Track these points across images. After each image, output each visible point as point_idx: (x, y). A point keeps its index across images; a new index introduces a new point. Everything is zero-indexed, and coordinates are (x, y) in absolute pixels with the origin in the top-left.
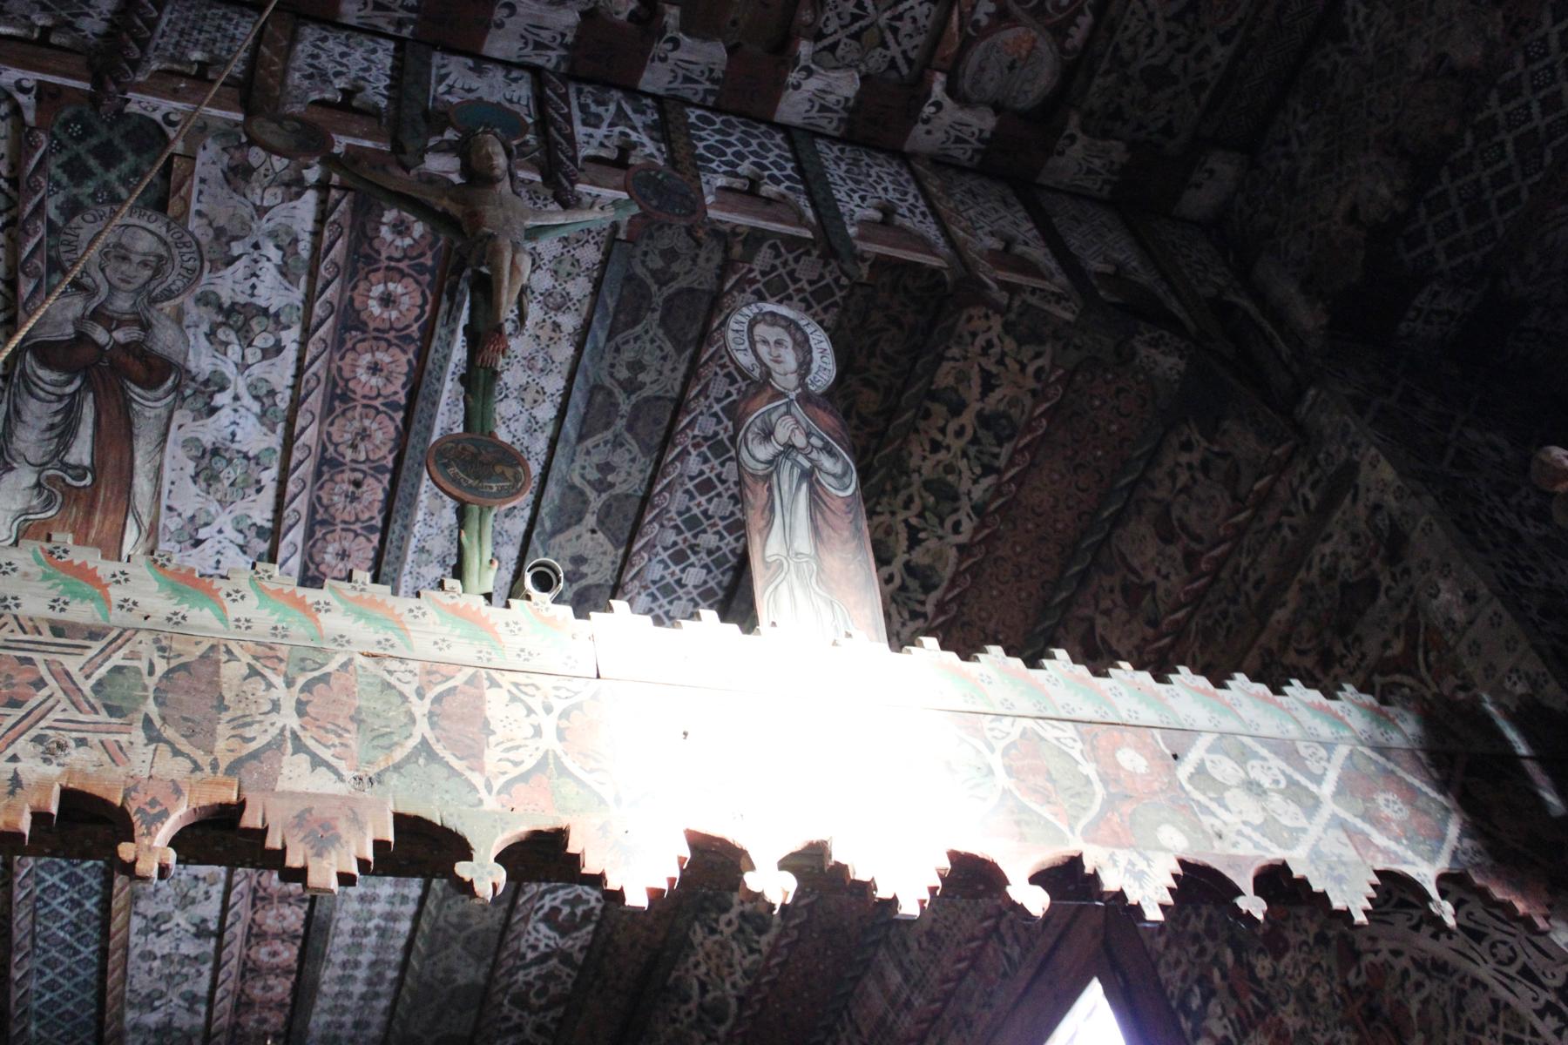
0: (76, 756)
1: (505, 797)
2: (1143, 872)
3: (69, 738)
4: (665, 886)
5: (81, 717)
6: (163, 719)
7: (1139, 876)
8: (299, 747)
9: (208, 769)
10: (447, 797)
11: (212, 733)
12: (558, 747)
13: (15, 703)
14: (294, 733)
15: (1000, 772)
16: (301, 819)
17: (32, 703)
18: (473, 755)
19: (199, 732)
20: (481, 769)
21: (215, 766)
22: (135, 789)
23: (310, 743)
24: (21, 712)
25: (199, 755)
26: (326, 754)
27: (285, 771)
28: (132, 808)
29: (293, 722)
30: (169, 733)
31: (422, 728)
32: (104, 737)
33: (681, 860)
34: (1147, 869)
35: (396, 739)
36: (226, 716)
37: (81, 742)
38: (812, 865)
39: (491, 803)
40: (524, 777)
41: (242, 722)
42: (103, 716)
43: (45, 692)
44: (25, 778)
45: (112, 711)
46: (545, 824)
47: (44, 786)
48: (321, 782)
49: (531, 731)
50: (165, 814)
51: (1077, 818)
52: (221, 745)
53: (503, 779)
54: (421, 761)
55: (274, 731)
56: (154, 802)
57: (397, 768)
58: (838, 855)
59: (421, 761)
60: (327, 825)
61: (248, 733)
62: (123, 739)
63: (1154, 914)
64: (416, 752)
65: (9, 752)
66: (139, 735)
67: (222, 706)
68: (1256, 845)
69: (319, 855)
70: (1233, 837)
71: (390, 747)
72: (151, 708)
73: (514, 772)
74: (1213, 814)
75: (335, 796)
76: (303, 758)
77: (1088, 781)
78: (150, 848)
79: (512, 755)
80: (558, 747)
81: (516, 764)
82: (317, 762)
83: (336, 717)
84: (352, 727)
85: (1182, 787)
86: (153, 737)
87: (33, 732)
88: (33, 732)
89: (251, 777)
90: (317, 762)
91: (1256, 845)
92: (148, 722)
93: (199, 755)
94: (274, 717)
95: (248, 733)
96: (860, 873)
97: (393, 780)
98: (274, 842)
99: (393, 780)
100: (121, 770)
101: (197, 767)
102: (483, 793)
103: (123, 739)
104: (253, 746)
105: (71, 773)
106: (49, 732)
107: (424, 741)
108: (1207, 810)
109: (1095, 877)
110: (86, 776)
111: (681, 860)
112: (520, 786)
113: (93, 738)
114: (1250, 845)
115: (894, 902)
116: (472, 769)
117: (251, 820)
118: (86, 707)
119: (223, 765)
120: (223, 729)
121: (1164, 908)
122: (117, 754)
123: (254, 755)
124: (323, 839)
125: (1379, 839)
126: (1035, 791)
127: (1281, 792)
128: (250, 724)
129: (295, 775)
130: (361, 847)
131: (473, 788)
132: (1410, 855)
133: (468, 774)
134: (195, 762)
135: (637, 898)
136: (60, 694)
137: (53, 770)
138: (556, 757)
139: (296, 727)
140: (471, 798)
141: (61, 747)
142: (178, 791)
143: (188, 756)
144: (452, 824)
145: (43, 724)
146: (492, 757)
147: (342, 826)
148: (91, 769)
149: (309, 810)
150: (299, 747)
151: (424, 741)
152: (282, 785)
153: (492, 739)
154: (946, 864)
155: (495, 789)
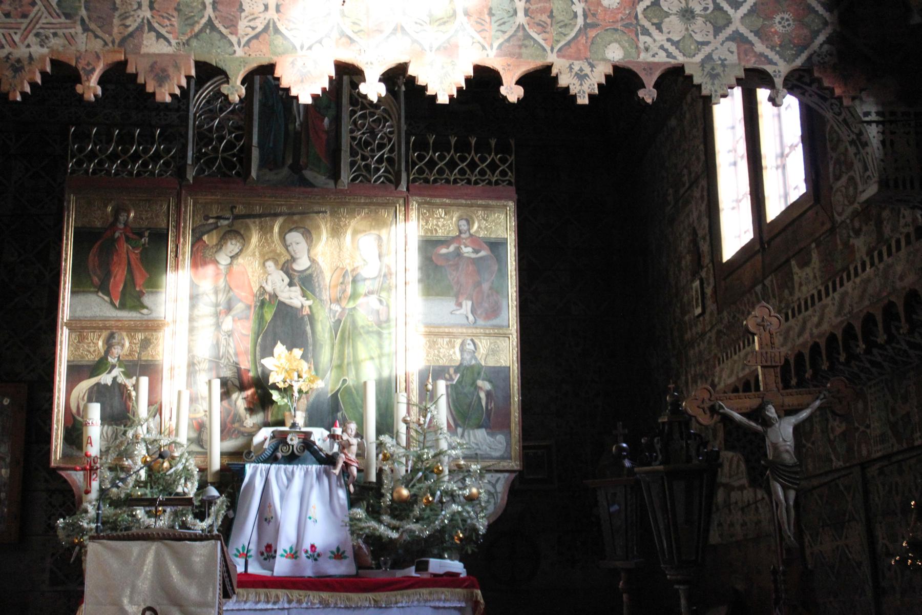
0: (54, 41)
1: (247, 48)
2: (586, 75)
3: (49, 32)
4: (320, 92)
5: (53, 21)
6: (89, 18)
7: (581, 76)
8: (151, 28)
9: (111, 45)
10: (219, 50)
11: (111, 23)
12: (275, 16)
13: (25, 16)
14: (148, 20)
15: (521, 14)
16: (152, 67)
17: (32, 15)
18: (232, 25)
19: (105, 23)
20: (236, 34)
21: (113, 42)
22: (80, 57)
23: (156, 25)
24: (27, 21)
25: (106, 37)
26: (163, 31)
27: (145, 42)
28: (80, 67)
29: (148, 14)
30: (92, 26)
31: (209, 11)
32: (65, 31)
33: (331, 78)
34: (589, 73)
35: (196, 19)
36: (117, 14)
37: (55, 35)
38: (397, 77)
39: (240, 52)
40: (256, 37)
41: (124, 17)
42: (63, 20)
43: (36, 8)
44: (35, 56)
45: (68, 16)
46: (265, 62)
47: (42, 58)
48: (162, 48)
49: (262, 8)
50: (93, 70)
51: (558, 41)
52: (115, 30)
53: (246, 38)
54: (208, 31)
55: (139, 20)
56: (88, 64)
57: (196, 36)
58: (411, 72)
59: (208, 31)
60: (164, 70)
61: (128, 22)
62: (72, 31)
63: (583, 100)
64: (206, 25)
65: (26, 43)
66: (79, 29)
67: (115, 9)
68: (669, 55)
69: (160, 86)
70: (656, 49)
71: (193, 25)
72: (83, 12)
73: (253, 33)
74: (650, 35)
75: (168, 55)
76: (153, 34)
77: (575, 15)
78: (89, 87)
79: (252, 24)
80: (275, 16)
81: (253, 29)
82: (159, 36)
83: (168, 9)
84: (175, 14)
85: (636, 17)
86: (86, 29)
87: (34, 31)
88: (34, 31)
89: (130, 45)
90: (159, 36)
91: (669, 55)
92: (83, 20)
93: (106, 37)
94: (139, 12)
95: (128, 22)
96: (421, 81)
97: (194, 43)
98: (141, 80)
99: (194, 43)
100: (73, 48)
101: (106, 44)
102: (236, 47)
103: (72, 31)
104: (131, 29)
105: (52, 51)
106: (41, 31)
107: (210, 19)
108: (646, 32)
109: (556, 78)
110: (59, 52)
111: (331, 78)
112: (254, 41)
113: (60, 32)
114: (663, 54)
115: (434, 97)
116: (231, 33)
117: (131, 69)
118: (55, 15)
119: (117, 41)
120: (116, 21)
121: (591, 96)
122: (70, 39)
123: (131, 35)
124: (162, 78)
125: (760, 47)
126: (539, 25)
127: (705, 17)
128: (127, 18)
129: (151, 46)
130: (179, 80)
131: (232, 45)
132: (775, 58)
133: (230, 37)
134: (104, 41)
135: (305, 99)
136: (43, 9)
137: (45, 50)
138: (274, 23)
139: (149, 17)
140: (230, 50)
141: (47, 38)
142: (98, 57)
143: (102, 39)
144: (221, 65)
145: (38, 26)
146: (242, 25)
147: (171, 71)
148: (61, 49)
149: (155, 63)
150: (151, 28)
151: (210, 19)
152: (144, 50)
153: (243, 15)
154: (471, 73)
155: (243, 43)
